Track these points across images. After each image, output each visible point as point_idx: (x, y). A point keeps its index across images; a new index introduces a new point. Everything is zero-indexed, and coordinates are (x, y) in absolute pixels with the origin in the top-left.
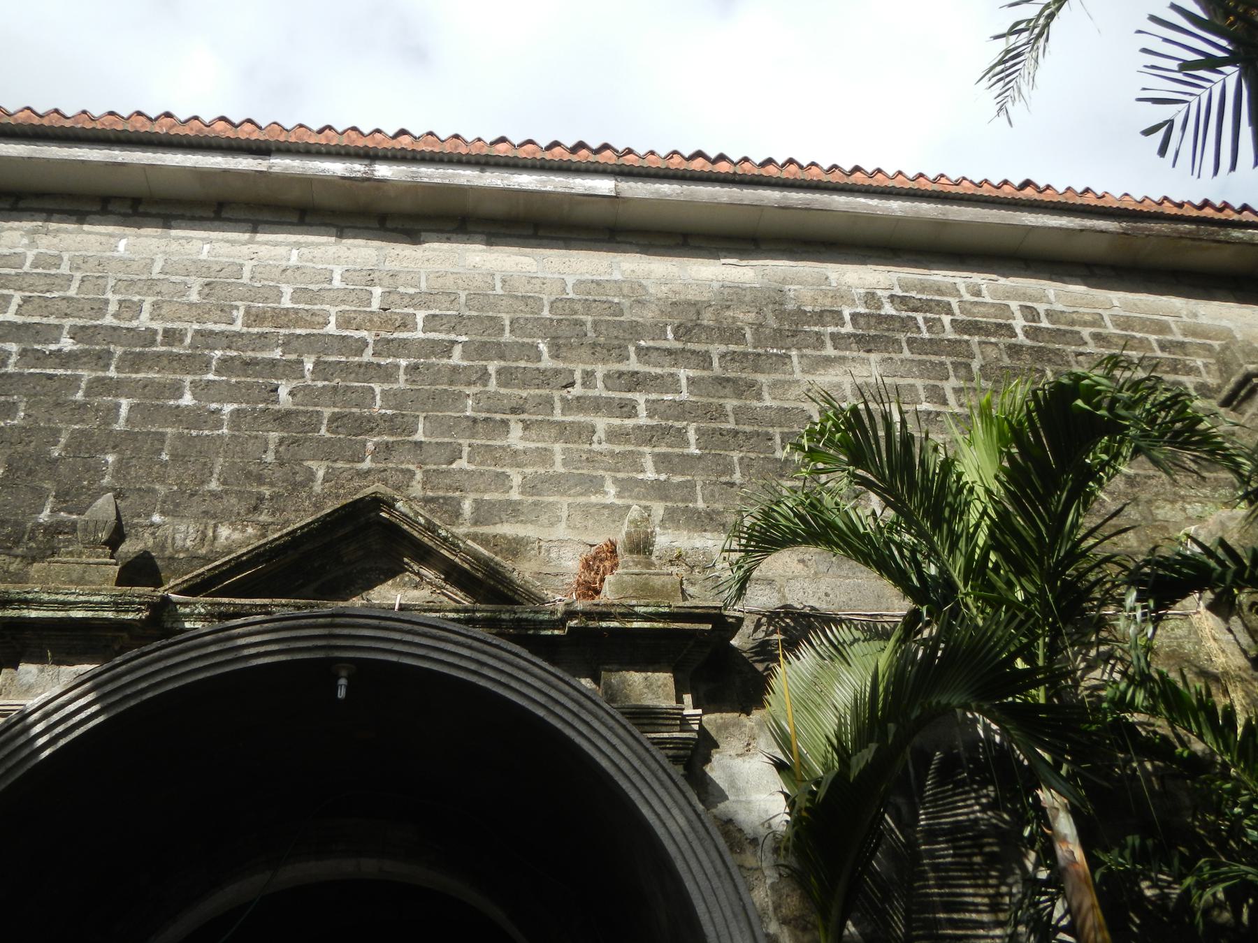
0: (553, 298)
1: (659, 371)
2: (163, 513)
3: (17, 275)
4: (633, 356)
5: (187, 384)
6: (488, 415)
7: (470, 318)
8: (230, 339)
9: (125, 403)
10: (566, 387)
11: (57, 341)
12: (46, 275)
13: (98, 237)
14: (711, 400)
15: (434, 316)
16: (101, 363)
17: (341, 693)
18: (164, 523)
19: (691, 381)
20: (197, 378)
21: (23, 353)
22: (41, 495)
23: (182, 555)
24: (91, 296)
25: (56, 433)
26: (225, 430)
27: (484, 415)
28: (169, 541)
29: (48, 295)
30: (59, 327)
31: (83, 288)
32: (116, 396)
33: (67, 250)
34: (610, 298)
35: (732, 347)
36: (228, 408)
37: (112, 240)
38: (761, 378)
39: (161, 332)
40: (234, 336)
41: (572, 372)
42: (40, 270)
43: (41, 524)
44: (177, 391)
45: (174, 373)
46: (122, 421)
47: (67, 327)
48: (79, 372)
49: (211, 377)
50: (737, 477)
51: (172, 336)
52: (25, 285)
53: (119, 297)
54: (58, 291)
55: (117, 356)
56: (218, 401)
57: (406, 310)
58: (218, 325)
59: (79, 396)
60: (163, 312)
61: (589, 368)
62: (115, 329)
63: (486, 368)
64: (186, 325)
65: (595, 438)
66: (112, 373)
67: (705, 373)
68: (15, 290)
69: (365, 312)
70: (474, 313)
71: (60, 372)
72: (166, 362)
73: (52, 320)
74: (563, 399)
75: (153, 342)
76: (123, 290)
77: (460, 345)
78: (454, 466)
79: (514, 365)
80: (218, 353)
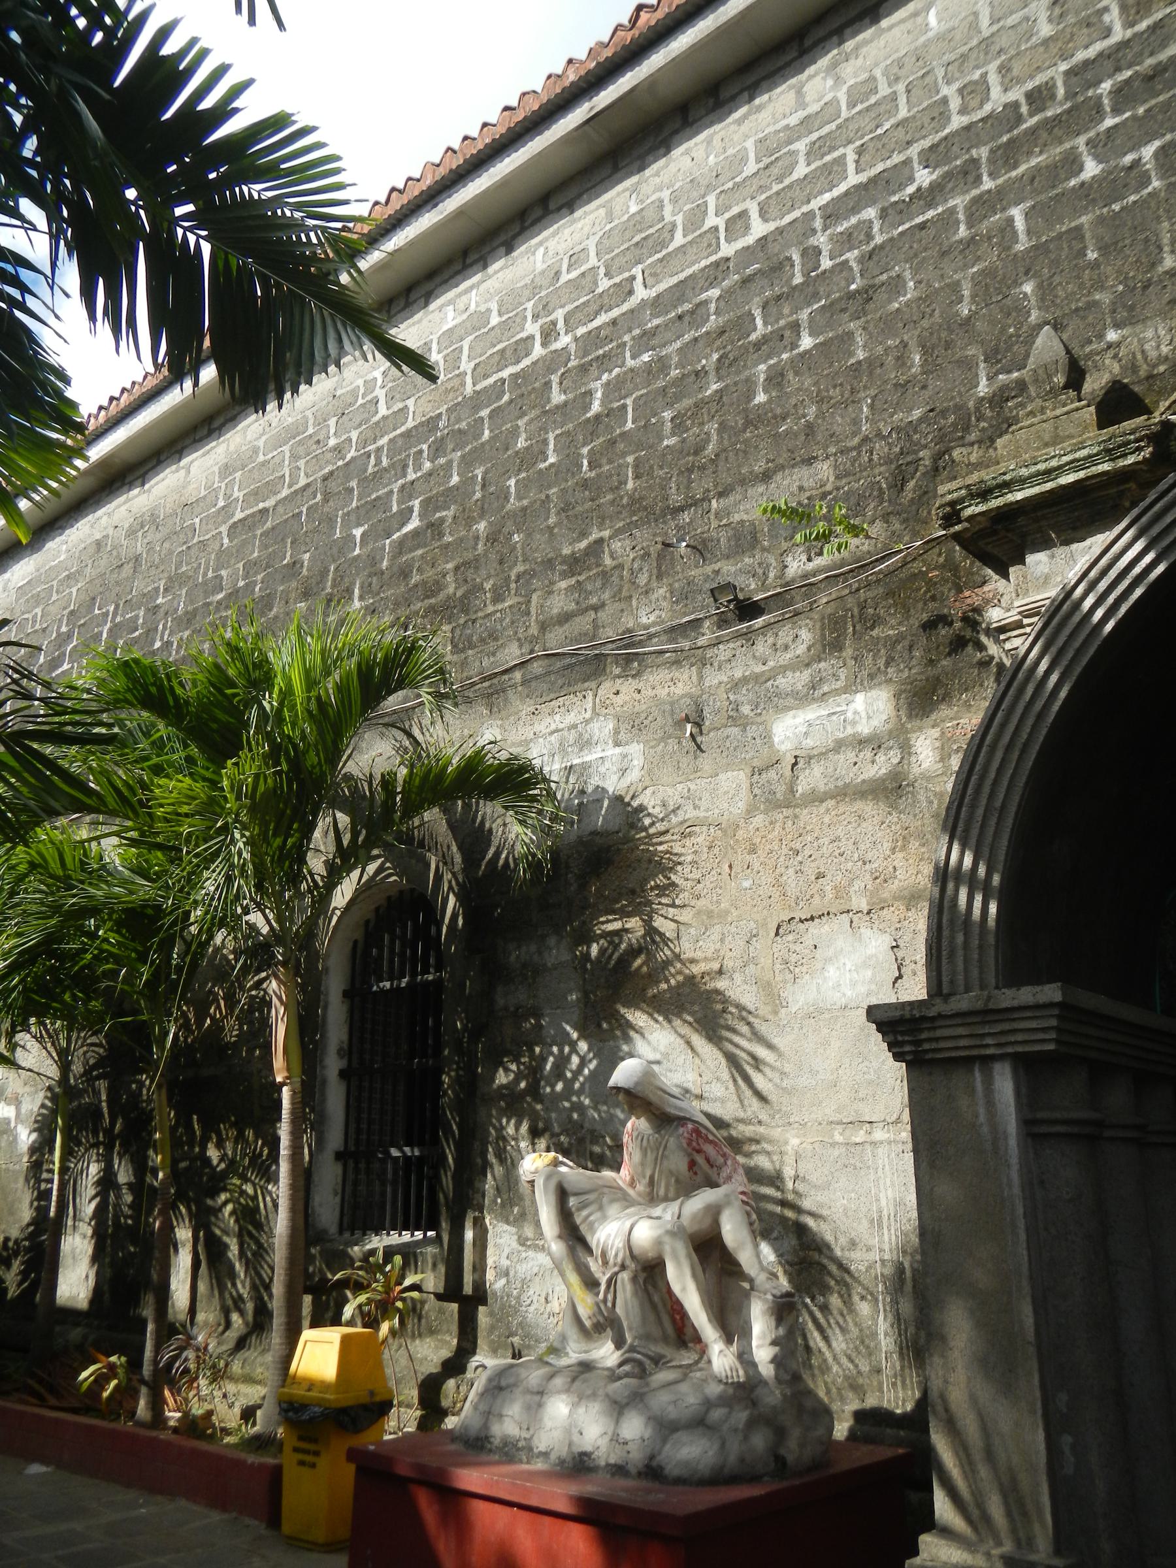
2: (1117, 326)
3: (839, 127)
5: (1082, 148)
8: (1114, 58)
9: (1017, 214)
11: (911, 179)
12: (868, 109)
13: (903, 27)
16: (970, 178)
18: (1124, 338)
20: (1092, 134)
21: (883, 214)
22: (968, 365)
23: (1162, 368)
24: (925, 104)
25: (955, 287)
26: (1156, 184)
28: (1139, 356)
29: (879, 131)
30: (907, 162)
31: (914, 100)
32: (1004, 209)
33: (876, 65)
36: (1148, 152)
37: (919, 20)
39: (1023, 101)
40: (1118, 50)
42: (859, 107)
43: (983, 399)
44: (1073, 163)
45: (1061, 143)
46: (1022, 237)
47: (915, 157)
48: (951, 203)
49: (1109, 122)
51: (1039, 98)
52: (852, 135)
53: (957, 85)
54: (887, 120)
55: (984, 160)
56: (1131, 150)
58: (1091, 49)
59: (963, 231)
60: (1015, 72)
62: (968, 128)
64: (1050, 73)
66: (988, 184)
68: (845, 146)
71: (930, 214)
72: (1045, 135)
73: (897, 159)
75: (1019, 119)
76: (957, 75)
80: (1106, 86)
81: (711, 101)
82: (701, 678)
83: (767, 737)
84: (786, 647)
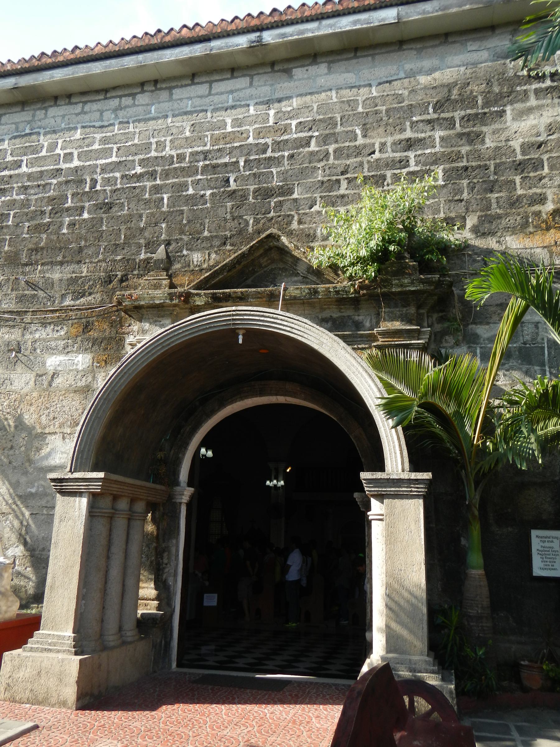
0: (364, 98)
1: (423, 135)
2: (187, 250)
3: (113, 135)
4: (408, 129)
5: (190, 182)
6: (329, 178)
7: (320, 120)
8: (206, 155)
9: (165, 196)
10: (370, 154)
11: (134, 169)
12: (125, 133)
13: (142, 107)
14: (453, 149)
15: (300, 123)
16: (153, 177)
17: (240, 341)
18: (188, 254)
19: (442, 139)
20: (193, 179)
21: (123, 177)
22: (139, 246)
23: (197, 269)
24: (144, 142)
25: (141, 216)
26: (208, 205)
27: (327, 178)
28: (191, 262)
29: (127, 144)
30: (134, 161)
31: (141, 138)
32: (162, 193)
33: (131, 117)
34: (397, 92)
35: (469, 111)
36: (208, 193)
37: (149, 107)
38: (484, 129)
39: (175, 156)
40: (207, 153)
41: (373, 145)
42: (121, 131)
43: (142, 260)
45: (184, 177)
46: (165, 206)
47: (137, 160)
48: (145, 183)
49: (199, 177)
50: (465, 196)
51: (181, 158)
52: (117, 141)
53: (156, 140)
54: (131, 141)
55: (159, 172)
56: (204, 190)
57: (286, 122)
58: (199, 148)
59: (147, 196)
60: (176, 144)
61: (383, 140)
62: (156, 158)
63: (327, 149)
64: (186, 150)
65: (385, 183)
66: (158, 182)
67: (452, 132)
68: (114, 144)
69: (267, 127)
70: (321, 117)
71: (138, 184)
72: (179, 172)
73: (130, 158)
74: (369, 162)
75: (172, 163)
76: (157, 136)
77: (315, 138)
78: (312, 210)
79: (343, 145)
80: (201, 163)
81: (67, 101)
82: (23, 335)
83: (44, 364)
84: (57, 331)
